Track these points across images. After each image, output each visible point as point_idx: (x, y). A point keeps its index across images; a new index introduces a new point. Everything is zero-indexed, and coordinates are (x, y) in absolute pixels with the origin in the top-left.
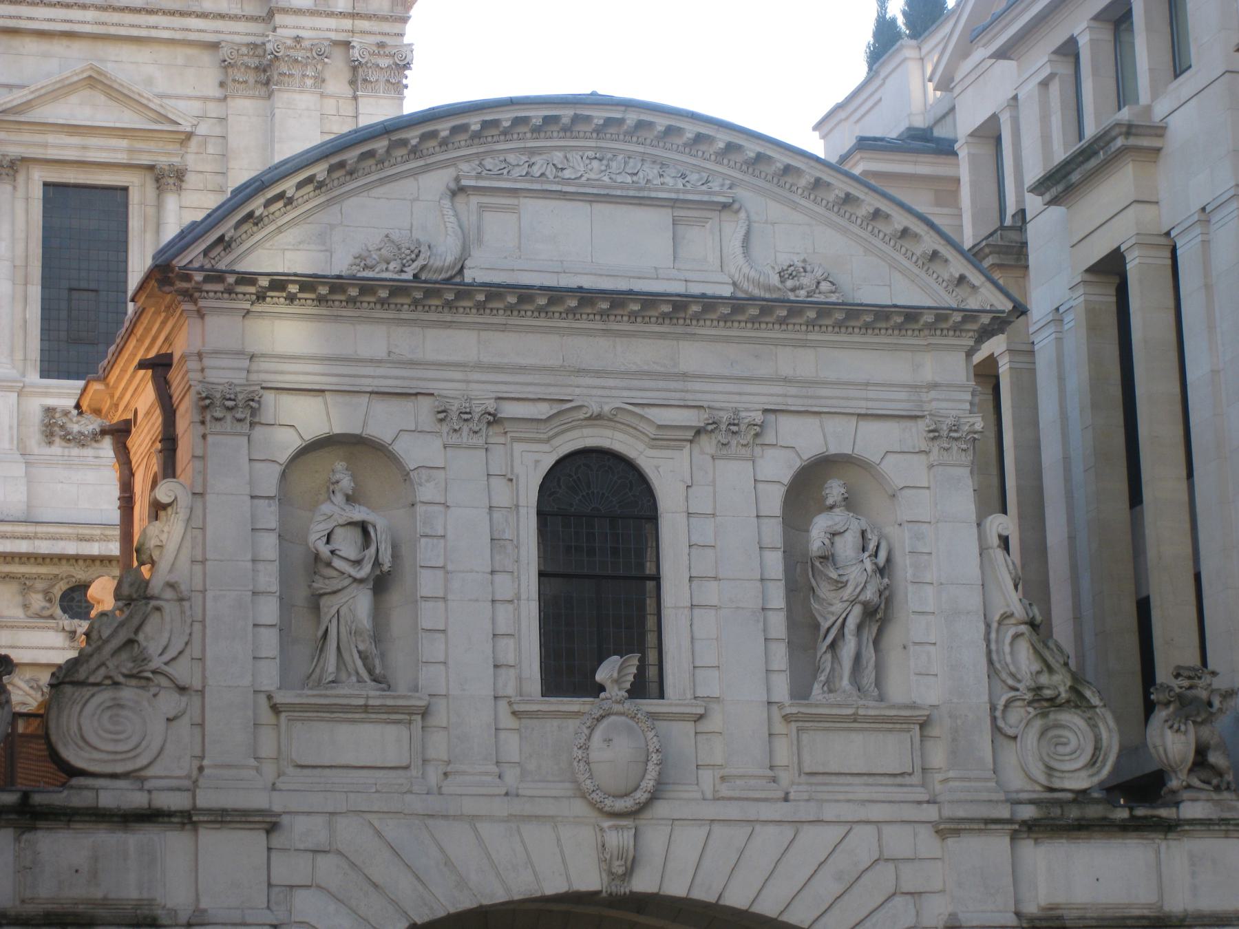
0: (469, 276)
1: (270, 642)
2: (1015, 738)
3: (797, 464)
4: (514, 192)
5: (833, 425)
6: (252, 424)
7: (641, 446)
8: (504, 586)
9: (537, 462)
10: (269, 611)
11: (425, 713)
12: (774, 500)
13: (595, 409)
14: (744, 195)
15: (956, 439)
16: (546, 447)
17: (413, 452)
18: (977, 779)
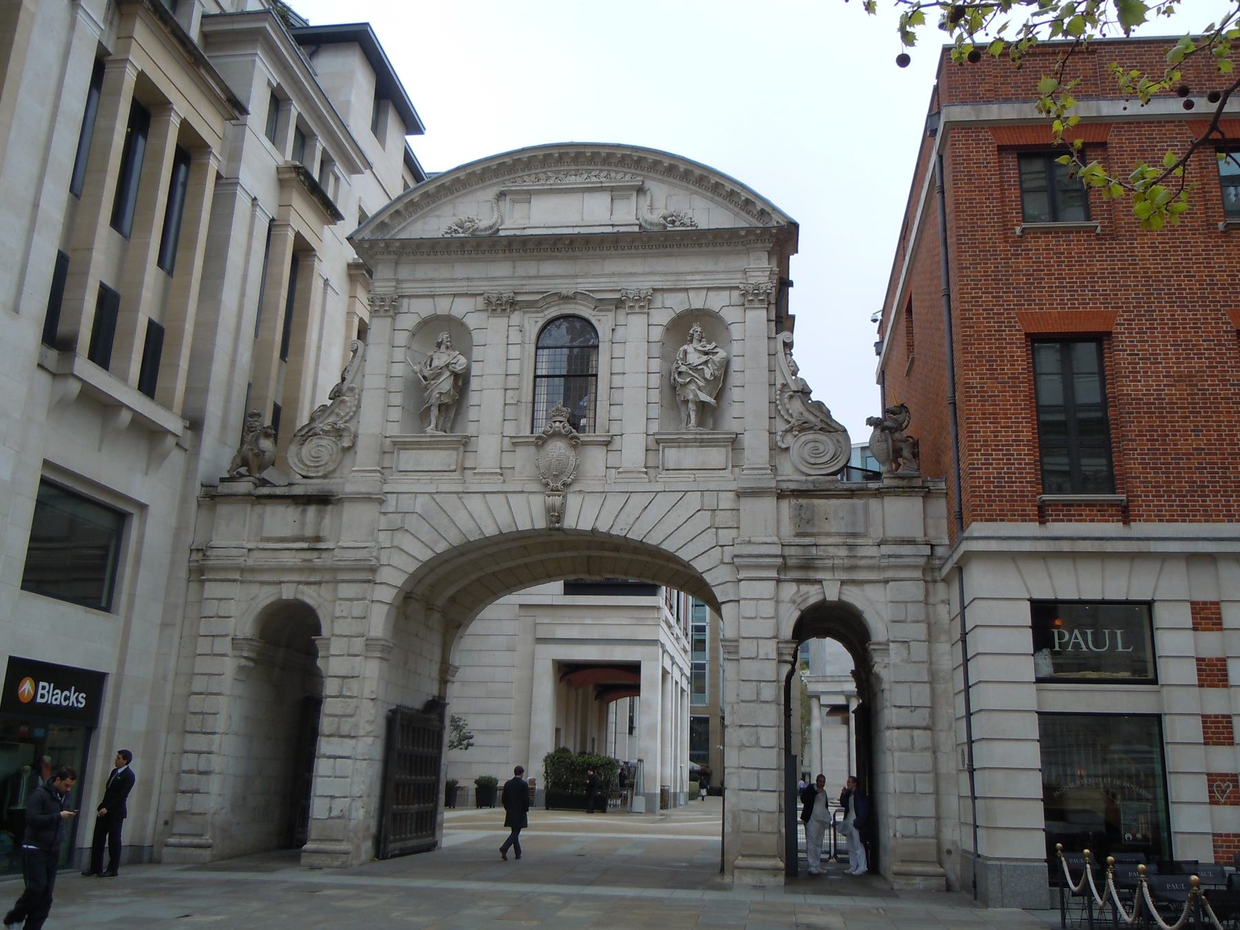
0: (502, 233)
1: (395, 414)
2: (787, 449)
3: (673, 315)
4: (529, 193)
5: (692, 294)
6: (396, 314)
7: (591, 311)
8: (512, 382)
9: (536, 322)
10: (397, 399)
11: (465, 444)
12: (657, 333)
13: (564, 292)
14: (649, 184)
15: (757, 295)
16: (542, 314)
17: (472, 321)
18: (761, 469)
